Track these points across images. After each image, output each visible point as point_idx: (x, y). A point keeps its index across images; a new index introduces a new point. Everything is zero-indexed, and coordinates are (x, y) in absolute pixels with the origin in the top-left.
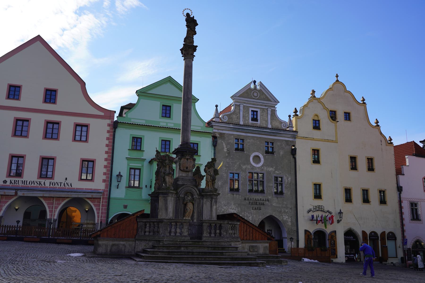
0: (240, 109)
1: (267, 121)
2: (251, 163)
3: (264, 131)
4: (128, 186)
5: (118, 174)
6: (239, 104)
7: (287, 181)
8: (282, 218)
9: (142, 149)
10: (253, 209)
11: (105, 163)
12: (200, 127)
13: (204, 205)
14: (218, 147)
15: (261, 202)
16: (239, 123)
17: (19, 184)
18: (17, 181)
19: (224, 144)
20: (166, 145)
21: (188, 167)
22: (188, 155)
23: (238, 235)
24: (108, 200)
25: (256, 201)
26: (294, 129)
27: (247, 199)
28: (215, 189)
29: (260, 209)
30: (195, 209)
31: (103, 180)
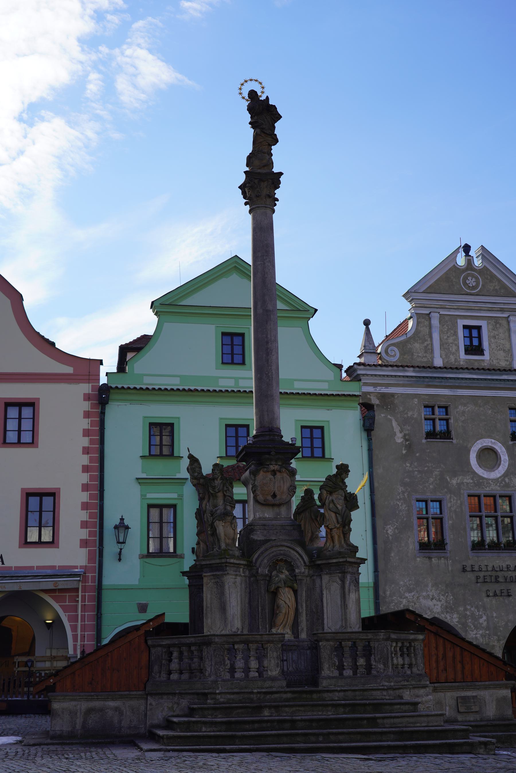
0: (430, 326)
2: (472, 468)
3: (504, 380)
4: (145, 552)
5: (118, 522)
6: (428, 312)
9: (176, 454)
10: (488, 596)
11: (85, 497)
13: (324, 592)
14: (378, 432)
16: (432, 362)
19: (394, 423)
20: (239, 438)
21: (277, 493)
22: (273, 463)
23: (420, 668)
24: (96, 594)
25: (494, 574)
27: (469, 569)
28: (350, 548)
29: (509, 596)
30: (302, 606)
31: (81, 540)
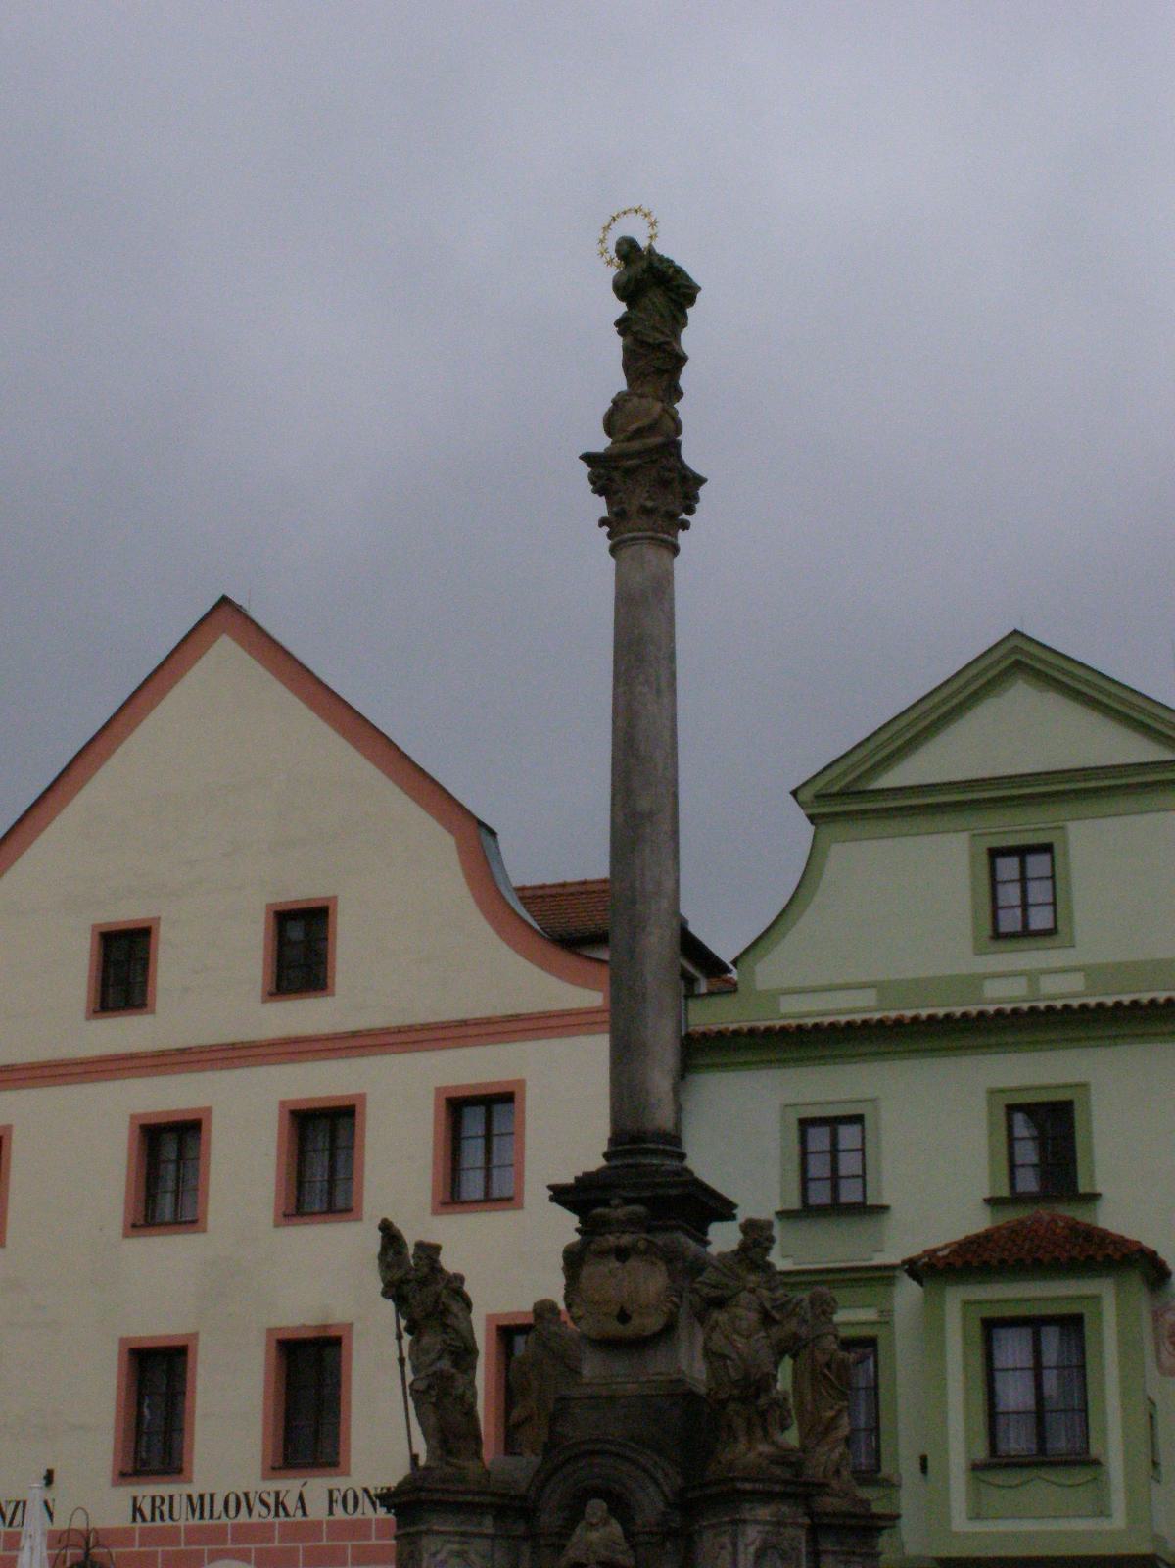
17: (176, 1516)
18: (163, 1501)
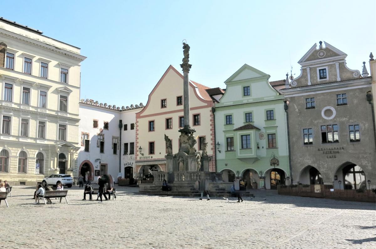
1: (336, 75)
3: (332, 86)
7: (364, 128)
8: (360, 163)
10: (328, 158)
12: (273, 96)
14: (290, 110)
15: (336, 150)
19: (295, 106)
26: (369, 75)
29: (335, 157)
